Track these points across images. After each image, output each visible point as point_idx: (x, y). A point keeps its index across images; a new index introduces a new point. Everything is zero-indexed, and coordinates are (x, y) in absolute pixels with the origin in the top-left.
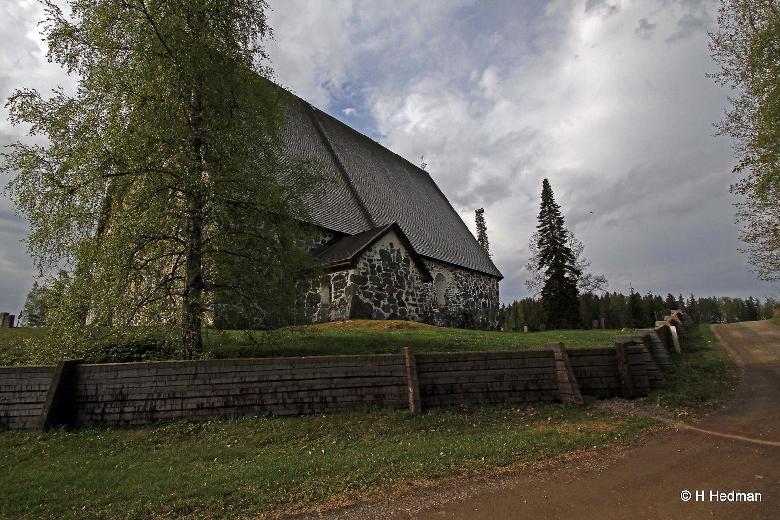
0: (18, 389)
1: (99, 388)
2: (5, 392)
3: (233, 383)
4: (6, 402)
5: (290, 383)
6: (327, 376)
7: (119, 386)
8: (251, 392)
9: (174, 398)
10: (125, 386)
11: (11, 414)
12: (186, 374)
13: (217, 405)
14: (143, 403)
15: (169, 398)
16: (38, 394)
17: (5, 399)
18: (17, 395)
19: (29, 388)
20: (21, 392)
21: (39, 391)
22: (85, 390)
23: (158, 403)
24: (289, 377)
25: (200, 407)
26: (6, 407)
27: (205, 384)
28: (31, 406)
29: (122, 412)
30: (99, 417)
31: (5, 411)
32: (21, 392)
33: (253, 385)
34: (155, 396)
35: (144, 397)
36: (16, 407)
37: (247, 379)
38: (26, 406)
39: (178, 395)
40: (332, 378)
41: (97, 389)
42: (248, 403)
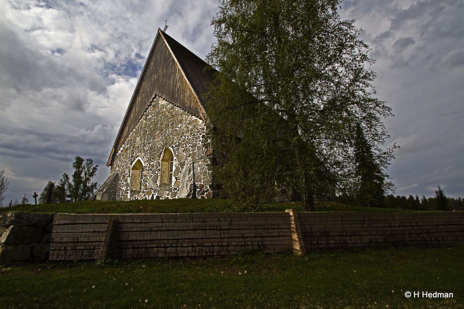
0: (266, 227)
1: (312, 227)
2: (259, 229)
3: (385, 227)
4: (261, 235)
5: (416, 228)
6: (435, 224)
7: (323, 226)
8: (396, 233)
9: (355, 235)
10: (327, 226)
11: (266, 243)
12: (358, 220)
13: (380, 240)
14: (339, 238)
15: (352, 235)
16: (279, 230)
17: (260, 234)
18: (266, 231)
19: (272, 227)
20: (268, 229)
21: (279, 229)
22: (305, 228)
23: (347, 238)
24: (415, 224)
25: (371, 242)
26: (262, 239)
27: (370, 227)
28: (276, 238)
29: (328, 244)
30: (316, 247)
31: (262, 241)
32: (268, 229)
33: (397, 228)
34: (345, 234)
35: (339, 234)
36: (267, 239)
37: (393, 225)
38: (273, 239)
39: (357, 234)
40: (438, 225)
41: (311, 228)
42: (397, 240)
